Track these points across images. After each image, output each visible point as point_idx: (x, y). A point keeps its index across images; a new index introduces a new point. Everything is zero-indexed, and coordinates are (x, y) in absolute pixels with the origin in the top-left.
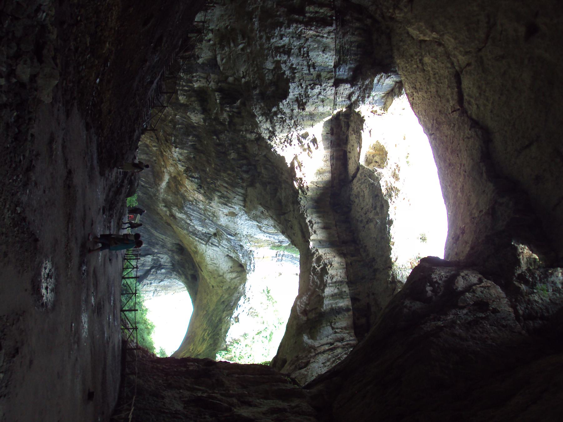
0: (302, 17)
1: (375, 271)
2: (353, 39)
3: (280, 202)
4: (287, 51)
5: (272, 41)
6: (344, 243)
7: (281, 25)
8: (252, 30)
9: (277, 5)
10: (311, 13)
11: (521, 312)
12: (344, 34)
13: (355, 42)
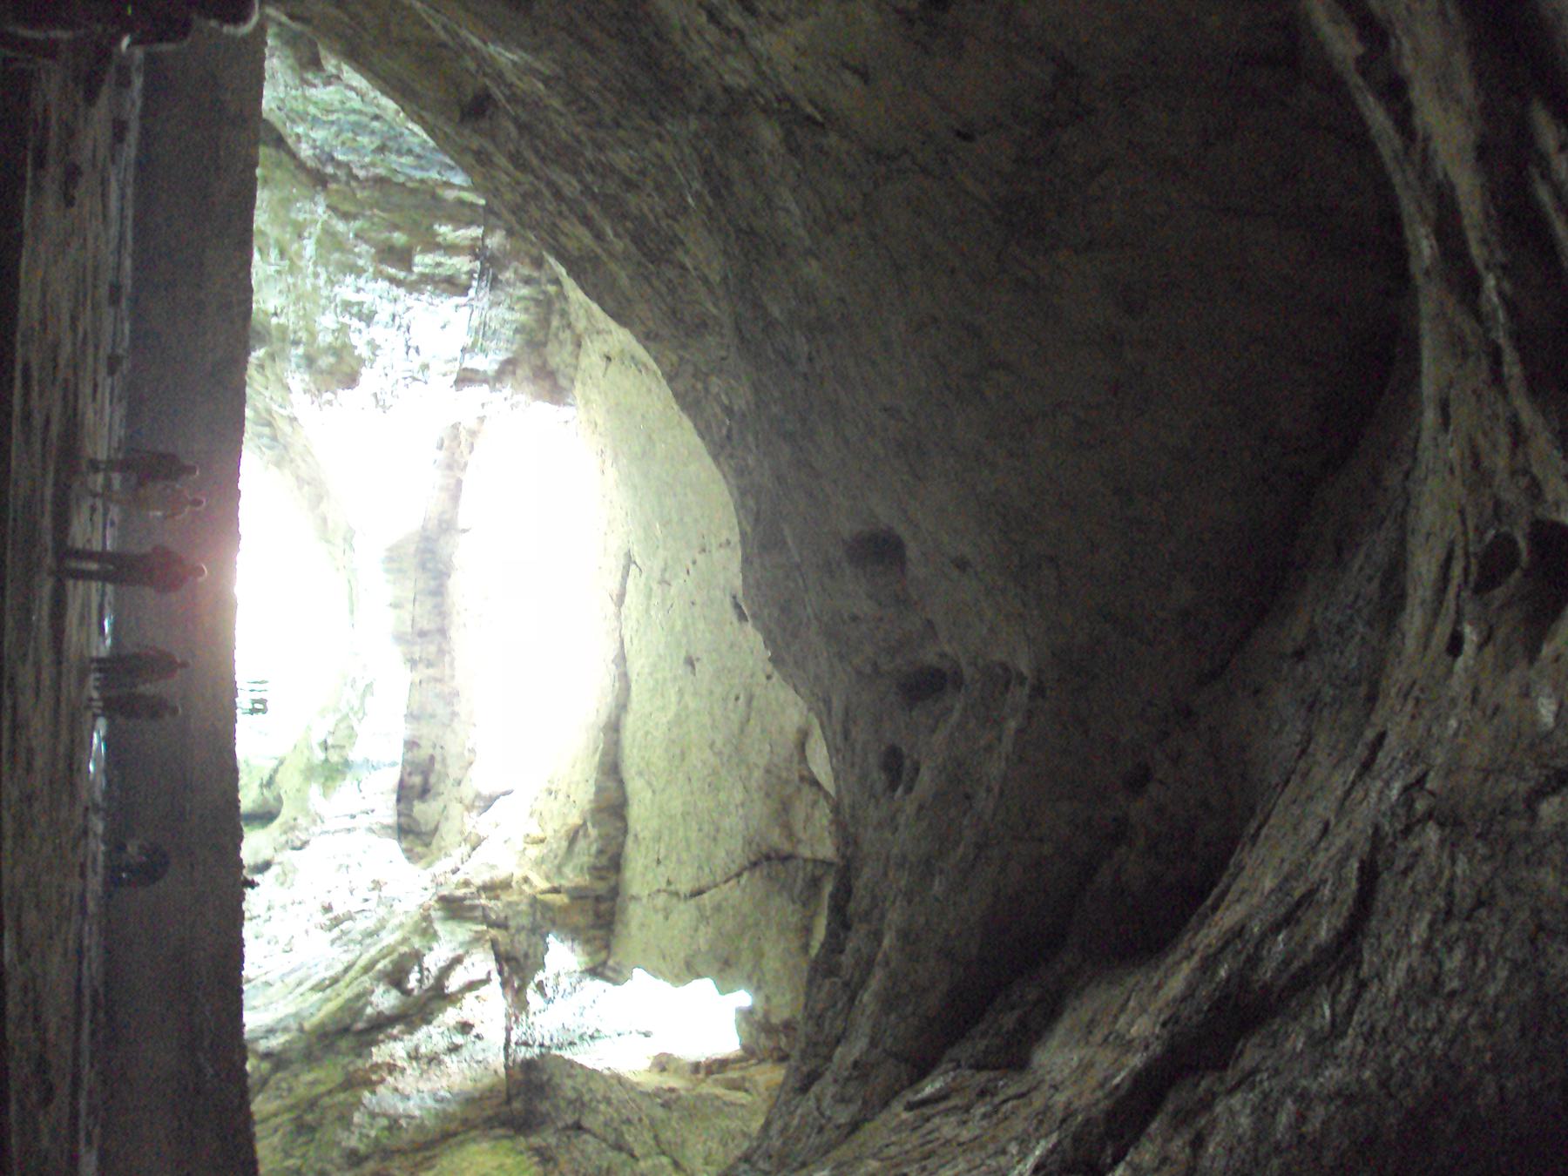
0: (402, 275)
1: (454, 714)
2: (508, 316)
3: (325, 520)
4: (368, 318)
5: (336, 289)
6: (422, 634)
7: (359, 272)
8: (301, 257)
9: (357, 236)
10: (426, 266)
11: (514, 1039)
12: (495, 304)
13: (513, 321)
